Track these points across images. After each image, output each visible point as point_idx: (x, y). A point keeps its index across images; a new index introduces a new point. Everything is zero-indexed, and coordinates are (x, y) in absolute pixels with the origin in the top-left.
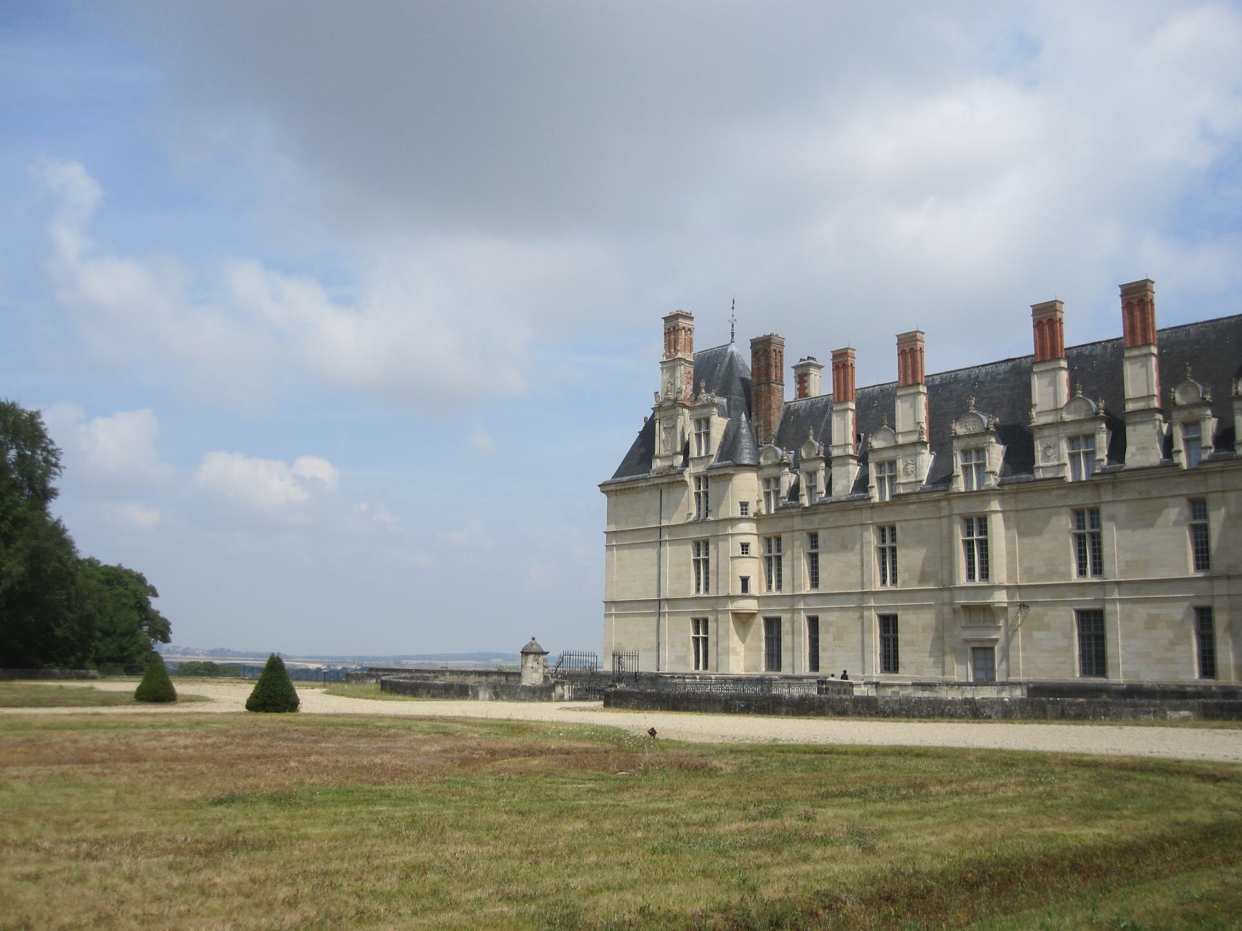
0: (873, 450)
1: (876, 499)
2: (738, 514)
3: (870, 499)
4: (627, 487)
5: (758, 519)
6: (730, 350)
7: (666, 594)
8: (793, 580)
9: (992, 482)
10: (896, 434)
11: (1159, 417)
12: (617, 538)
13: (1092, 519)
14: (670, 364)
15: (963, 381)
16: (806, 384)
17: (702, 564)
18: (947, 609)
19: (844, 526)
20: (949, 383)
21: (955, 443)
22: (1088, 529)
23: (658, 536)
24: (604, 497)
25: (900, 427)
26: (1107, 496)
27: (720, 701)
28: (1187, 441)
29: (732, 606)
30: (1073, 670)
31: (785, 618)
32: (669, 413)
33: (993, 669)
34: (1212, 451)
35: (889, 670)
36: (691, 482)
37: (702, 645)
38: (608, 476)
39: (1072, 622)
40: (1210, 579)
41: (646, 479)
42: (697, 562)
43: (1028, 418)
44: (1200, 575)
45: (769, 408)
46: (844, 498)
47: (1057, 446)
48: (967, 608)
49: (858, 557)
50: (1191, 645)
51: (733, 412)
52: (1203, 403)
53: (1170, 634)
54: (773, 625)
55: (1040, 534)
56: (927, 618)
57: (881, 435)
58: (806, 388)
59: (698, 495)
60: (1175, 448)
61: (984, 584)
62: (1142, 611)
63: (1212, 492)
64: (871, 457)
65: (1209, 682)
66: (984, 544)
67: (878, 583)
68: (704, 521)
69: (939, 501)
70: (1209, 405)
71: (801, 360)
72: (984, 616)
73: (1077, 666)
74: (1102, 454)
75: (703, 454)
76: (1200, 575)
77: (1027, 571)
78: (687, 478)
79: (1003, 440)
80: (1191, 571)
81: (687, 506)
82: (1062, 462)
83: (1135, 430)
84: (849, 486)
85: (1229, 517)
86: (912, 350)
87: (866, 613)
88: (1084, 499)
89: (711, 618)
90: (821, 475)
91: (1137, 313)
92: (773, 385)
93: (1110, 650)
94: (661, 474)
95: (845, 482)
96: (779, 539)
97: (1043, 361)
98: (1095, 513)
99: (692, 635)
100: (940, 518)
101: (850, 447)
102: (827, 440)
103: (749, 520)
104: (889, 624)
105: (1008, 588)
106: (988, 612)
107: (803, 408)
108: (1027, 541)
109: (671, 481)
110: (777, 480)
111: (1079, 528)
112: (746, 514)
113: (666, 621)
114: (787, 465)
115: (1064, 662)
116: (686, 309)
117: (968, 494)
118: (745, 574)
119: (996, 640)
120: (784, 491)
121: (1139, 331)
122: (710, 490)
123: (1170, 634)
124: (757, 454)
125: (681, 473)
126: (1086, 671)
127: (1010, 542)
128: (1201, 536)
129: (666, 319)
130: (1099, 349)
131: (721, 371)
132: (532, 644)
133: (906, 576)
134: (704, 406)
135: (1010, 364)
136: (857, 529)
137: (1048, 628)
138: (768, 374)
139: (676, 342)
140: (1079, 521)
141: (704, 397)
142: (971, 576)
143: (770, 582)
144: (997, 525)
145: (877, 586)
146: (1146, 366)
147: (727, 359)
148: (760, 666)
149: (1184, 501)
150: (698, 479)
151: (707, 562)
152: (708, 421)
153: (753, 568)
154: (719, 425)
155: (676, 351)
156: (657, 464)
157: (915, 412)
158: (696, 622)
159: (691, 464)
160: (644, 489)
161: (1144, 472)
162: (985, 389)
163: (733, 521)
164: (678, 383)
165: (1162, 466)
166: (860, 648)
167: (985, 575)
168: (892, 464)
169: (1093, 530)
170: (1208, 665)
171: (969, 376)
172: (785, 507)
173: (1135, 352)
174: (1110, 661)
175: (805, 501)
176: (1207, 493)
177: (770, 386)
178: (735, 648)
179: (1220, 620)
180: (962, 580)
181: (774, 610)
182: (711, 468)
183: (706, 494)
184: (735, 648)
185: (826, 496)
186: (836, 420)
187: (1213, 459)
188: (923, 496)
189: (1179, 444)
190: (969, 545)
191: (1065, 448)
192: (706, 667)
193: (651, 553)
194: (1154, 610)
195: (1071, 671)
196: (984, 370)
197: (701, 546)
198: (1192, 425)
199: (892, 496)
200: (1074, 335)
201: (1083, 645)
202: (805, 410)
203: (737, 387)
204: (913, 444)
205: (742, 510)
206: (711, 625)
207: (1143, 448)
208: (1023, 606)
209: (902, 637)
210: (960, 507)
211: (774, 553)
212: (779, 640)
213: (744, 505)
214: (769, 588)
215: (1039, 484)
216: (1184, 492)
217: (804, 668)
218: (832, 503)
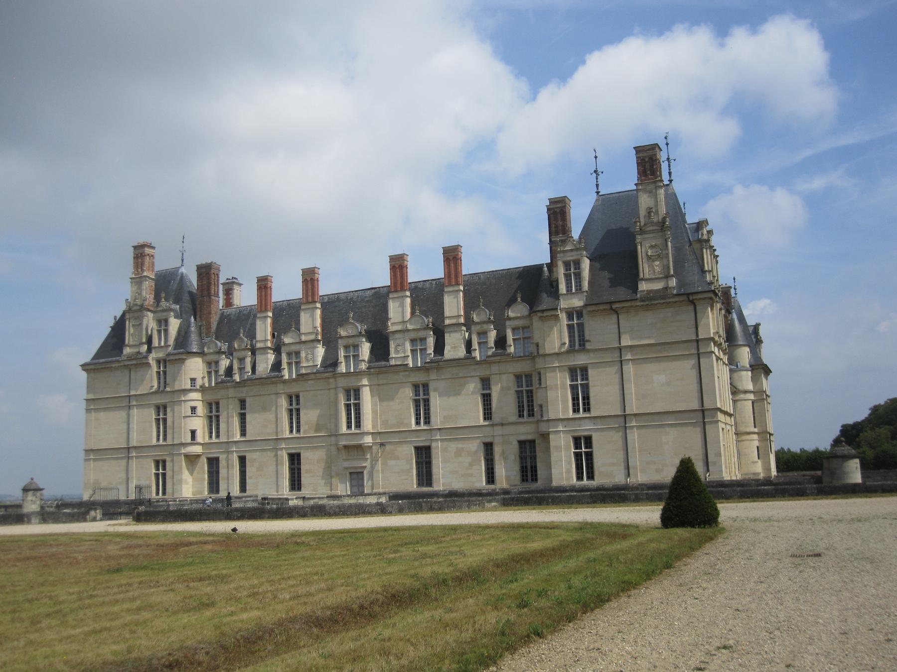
0: (285, 345)
1: (287, 377)
2: (188, 386)
3: (282, 376)
5: (203, 389)
6: (180, 271)
7: (134, 443)
8: (228, 431)
9: (363, 366)
10: (300, 334)
11: (464, 328)
12: (94, 404)
13: (424, 391)
14: (138, 280)
15: (343, 300)
16: (231, 296)
17: (162, 422)
18: (333, 448)
19: (263, 395)
20: (333, 302)
21: (340, 341)
22: (422, 396)
23: (127, 402)
25: (303, 329)
26: (433, 376)
27: (223, 513)
28: (479, 344)
29: (184, 451)
30: (413, 484)
31: (222, 457)
32: (136, 315)
33: (363, 485)
34: (494, 350)
35: (527, 480)
36: (153, 364)
37: (161, 479)
38: (88, 358)
39: (412, 454)
40: (492, 425)
41: (118, 361)
42: (158, 420)
43: (386, 327)
44: (486, 423)
45: (210, 313)
46: (264, 376)
47: (403, 344)
48: (346, 447)
49: (274, 415)
50: (481, 466)
51: (184, 315)
52: (489, 321)
53: (469, 459)
54: (213, 463)
55: (392, 399)
56: (320, 454)
57: (290, 334)
58: (231, 299)
59: (158, 373)
60: (473, 348)
61: (358, 431)
62: (453, 446)
63: (493, 374)
64: (283, 349)
65: (492, 487)
66: (358, 407)
67: (288, 432)
68: (163, 392)
69: (329, 378)
70: (492, 322)
71: (227, 279)
72: (357, 452)
73: (415, 481)
74: (431, 350)
75: (163, 344)
76: (486, 423)
77: (385, 423)
78: (151, 361)
79: (369, 340)
80: (481, 422)
81: (150, 380)
82: (406, 354)
83: (450, 336)
84: (268, 368)
85: (502, 389)
86: (312, 279)
87: (279, 453)
88: (420, 378)
89: (168, 459)
90: (248, 360)
91: (452, 265)
92: (213, 297)
93: (434, 470)
94: (130, 357)
95: (265, 365)
96: (217, 404)
97: (396, 291)
98: (426, 386)
99: (154, 471)
100: (329, 389)
101: (269, 342)
102: (252, 335)
103: (196, 390)
104: (295, 459)
105: (372, 433)
106: (360, 449)
107: (234, 313)
108: (384, 404)
109: (139, 362)
110: (217, 363)
111: (416, 396)
112: (194, 386)
113: (134, 463)
114: (224, 353)
115: (407, 479)
116: (148, 240)
117: (348, 374)
118: (194, 428)
119: (365, 467)
120: (222, 371)
121: (453, 276)
122: (168, 369)
123: (469, 459)
124: (202, 345)
125: (146, 357)
126: (420, 484)
127: (374, 404)
128: (487, 399)
129: (135, 247)
130: (427, 285)
131: (174, 285)
132: (31, 483)
133: (307, 427)
134: (163, 311)
135: (373, 291)
136: (273, 397)
137: (397, 458)
138: (209, 289)
139: (142, 264)
140: (416, 391)
141: (164, 304)
142: (349, 426)
143: (211, 433)
144: (366, 395)
145: (287, 434)
146: (457, 297)
147: (179, 278)
148: (204, 491)
149: (477, 379)
150: (158, 362)
151: (165, 420)
152: (166, 321)
153: (199, 424)
154: (174, 324)
155: (142, 270)
156: (127, 351)
157: (314, 320)
158: (157, 463)
159: (153, 351)
160: (117, 368)
161: (455, 362)
162: (357, 306)
163: (185, 391)
164: (144, 293)
165: (466, 358)
167: (358, 425)
168: (298, 353)
169: (425, 397)
170: (491, 478)
171: (347, 298)
172: (223, 382)
173: (451, 289)
174: (434, 477)
175: (237, 378)
176: (491, 375)
177: (210, 298)
178: (186, 479)
179: (497, 450)
180: (344, 429)
181: (214, 453)
182: (169, 355)
183: (165, 372)
184: (186, 479)
185: (252, 374)
186: (259, 323)
187: (494, 355)
188: (318, 376)
189: (475, 345)
190: (348, 407)
191: (408, 347)
192: (164, 493)
193: (122, 414)
194: (460, 445)
195: (412, 485)
196: (356, 294)
197: (161, 409)
198: (483, 334)
199: (298, 375)
200: (414, 275)
201: (418, 468)
203: (186, 297)
204: (312, 341)
205: (191, 383)
206: (168, 465)
207: (455, 347)
208: (382, 444)
209: (303, 467)
210: (343, 383)
211: (214, 413)
212: (218, 472)
213: (193, 380)
214: (211, 437)
215: (392, 368)
216: (479, 374)
217: (236, 491)
218: (256, 379)
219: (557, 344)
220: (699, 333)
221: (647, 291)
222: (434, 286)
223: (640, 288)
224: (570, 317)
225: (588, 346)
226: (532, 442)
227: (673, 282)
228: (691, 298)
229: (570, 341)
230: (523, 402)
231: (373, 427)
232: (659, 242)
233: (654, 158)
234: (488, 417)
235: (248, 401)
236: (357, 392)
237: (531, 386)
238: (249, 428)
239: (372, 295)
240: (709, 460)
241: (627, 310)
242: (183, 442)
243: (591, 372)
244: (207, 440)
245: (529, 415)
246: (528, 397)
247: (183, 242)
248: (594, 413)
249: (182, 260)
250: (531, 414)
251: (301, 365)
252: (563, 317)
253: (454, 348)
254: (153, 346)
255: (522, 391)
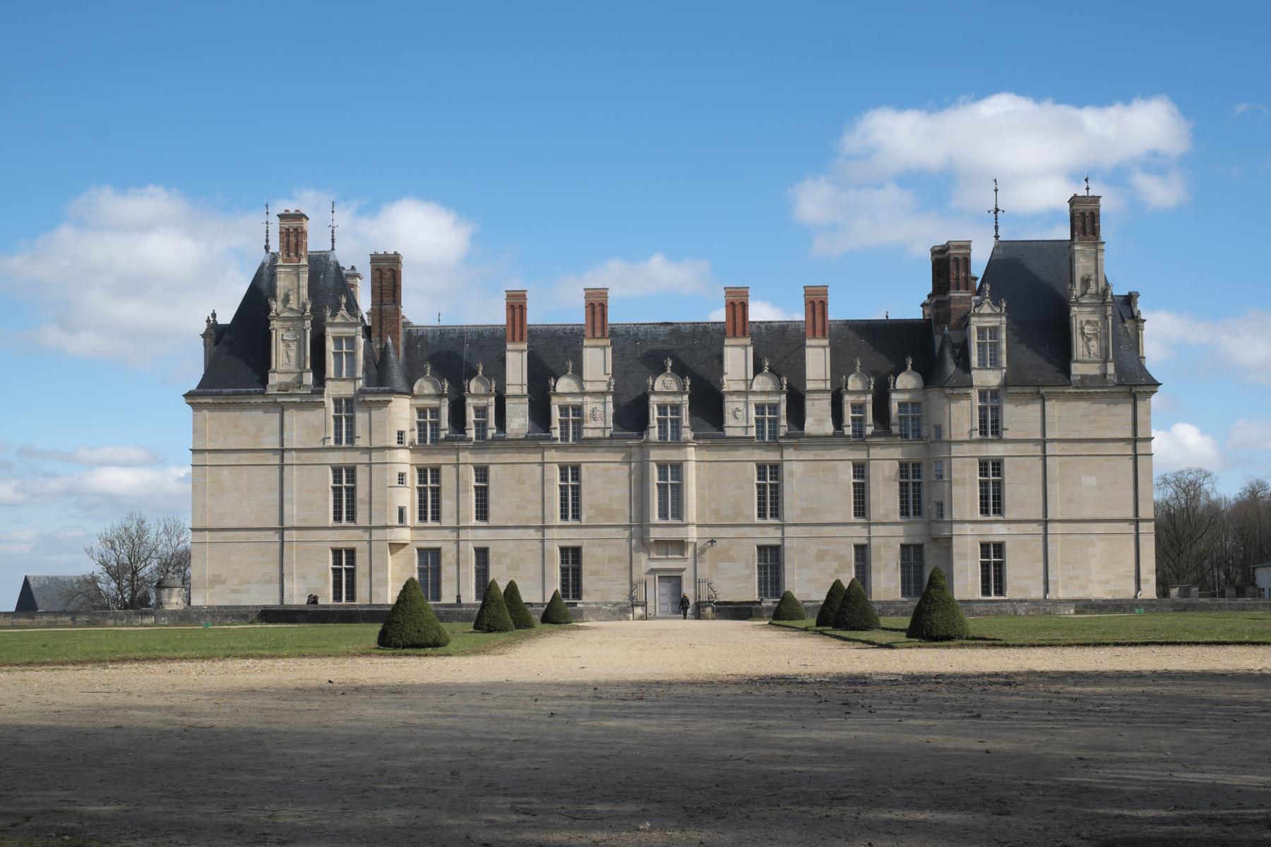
1: (559, 442)
4: (231, 401)
5: (414, 449)
15: (622, 336)
24: (189, 408)
25: (587, 374)
26: (789, 454)
30: (754, 593)
38: (193, 385)
39: (754, 555)
43: (721, 385)
50: (851, 573)
62: (813, 548)
66: (678, 489)
78: (325, 400)
82: (750, 424)
83: (813, 405)
97: (735, 335)
106: (680, 545)
119: (683, 570)
137: (732, 560)
147: (332, 269)
150: (337, 401)
159: (329, 384)
160: (256, 407)
161: (820, 441)
165: (834, 435)
166: (541, 577)
171: (628, 332)
175: (472, 433)
181: (431, 539)
185: (498, 432)
191: (753, 413)
202: (434, 338)
205: (398, 438)
206: (361, 559)
219: (967, 428)
220: (1139, 432)
221: (1082, 376)
222: (763, 331)
223: (1074, 371)
224: (983, 395)
225: (1006, 435)
226: (919, 547)
227: (1111, 369)
228: (1134, 391)
229: (981, 427)
230: (914, 496)
231: (698, 517)
232: (1095, 318)
233: (1096, 214)
234: (859, 513)
235: (493, 471)
236: (678, 468)
237: (919, 477)
238: (493, 508)
239: (670, 334)
240: (1142, 578)
241: (1056, 396)
242: (389, 524)
243: (1007, 467)
244: (417, 523)
245: (915, 514)
246: (914, 491)
247: (333, 212)
248: (1008, 515)
249: (333, 241)
250: (918, 512)
251: (585, 425)
252: (975, 394)
253: (818, 418)
254: (327, 376)
255: (907, 484)
